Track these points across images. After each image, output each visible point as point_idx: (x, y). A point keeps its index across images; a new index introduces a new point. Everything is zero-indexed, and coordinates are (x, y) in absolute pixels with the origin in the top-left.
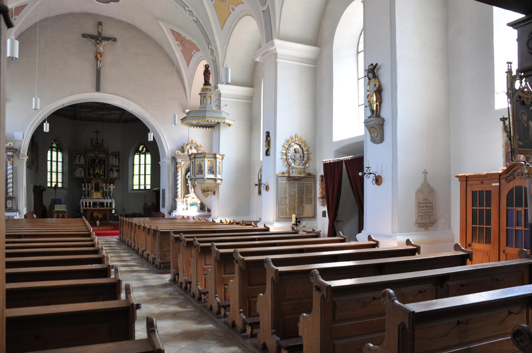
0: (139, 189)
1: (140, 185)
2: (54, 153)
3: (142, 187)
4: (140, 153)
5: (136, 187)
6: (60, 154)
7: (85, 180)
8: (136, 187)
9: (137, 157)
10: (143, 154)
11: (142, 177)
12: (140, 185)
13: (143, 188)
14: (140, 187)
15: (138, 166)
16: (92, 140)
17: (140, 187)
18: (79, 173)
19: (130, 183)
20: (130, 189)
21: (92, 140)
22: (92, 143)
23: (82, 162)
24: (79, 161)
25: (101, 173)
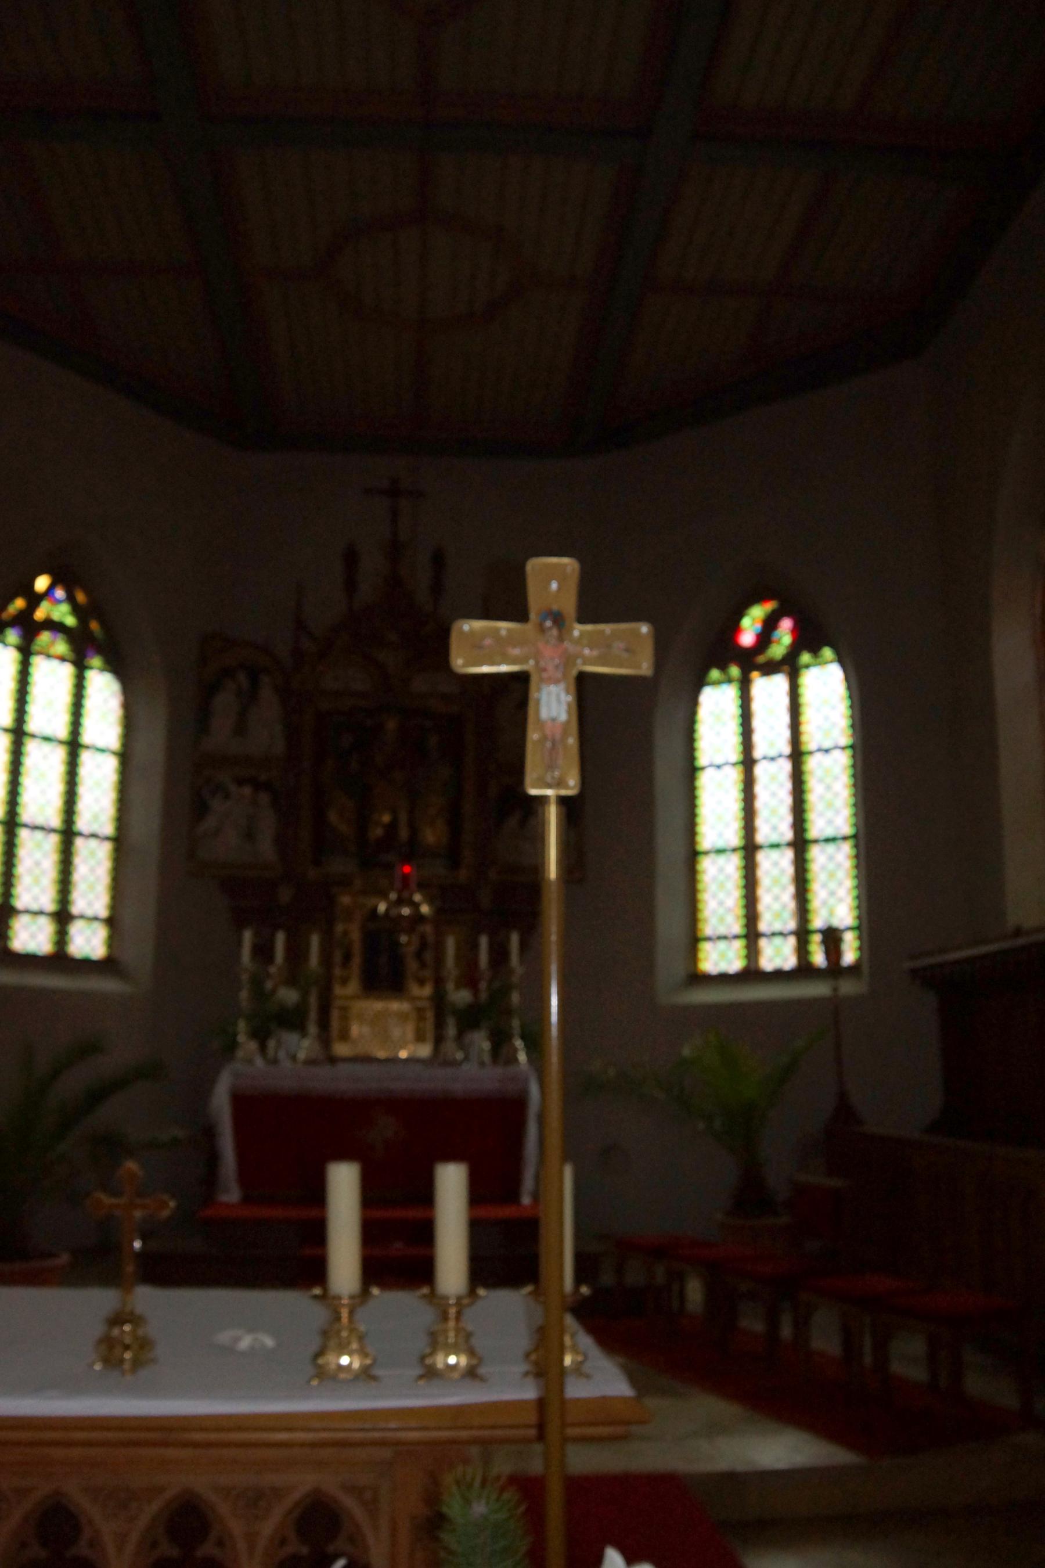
0: (751, 974)
1: (752, 935)
2: (52, 676)
3: (780, 955)
4: (751, 662)
5: (720, 957)
6: (104, 690)
7: (285, 895)
8: (720, 957)
9: (716, 704)
10: (770, 669)
11: (775, 868)
12: (752, 935)
13: (789, 961)
14: (752, 951)
15: (734, 776)
16: (351, 558)
17: (752, 951)
18: (244, 831)
19: (668, 926)
20: (668, 968)
21: (351, 558)
22: (351, 585)
23: (267, 733)
24: (240, 729)
25: (432, 836)
